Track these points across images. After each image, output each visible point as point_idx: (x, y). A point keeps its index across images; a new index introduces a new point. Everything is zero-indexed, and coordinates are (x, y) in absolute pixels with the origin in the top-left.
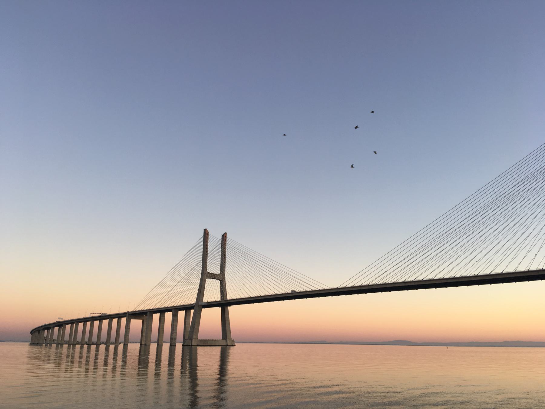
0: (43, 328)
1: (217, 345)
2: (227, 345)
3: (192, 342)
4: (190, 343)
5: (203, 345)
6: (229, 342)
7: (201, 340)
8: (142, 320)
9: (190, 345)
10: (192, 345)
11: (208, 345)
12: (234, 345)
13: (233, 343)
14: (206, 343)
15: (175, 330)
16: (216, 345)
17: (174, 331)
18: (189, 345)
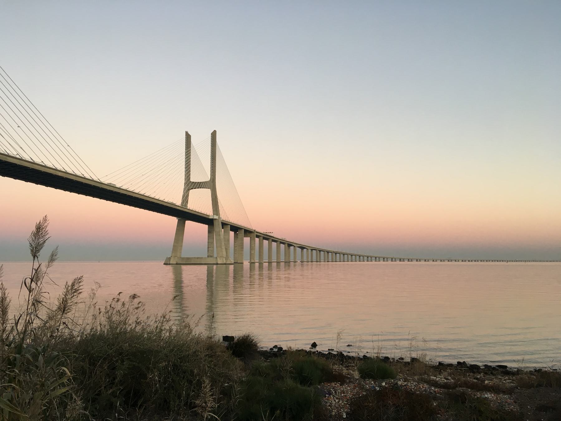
0: (300, 246)
1: (204, 263)
2: (217, 264)
3: (169, 262)
4: (169, 262)
5: (185, 263)
6: (220, 260)
7: (183, 258)
8: (250, 238)
9: (168, 263)
10: (170, 263)
11: (192, 263)
12: (227, 263)
13: (227, 261)
14: (189, 262)
15: (210, 247)
16: (202, 263)
17: (209, 249)
18: (167, 263)
